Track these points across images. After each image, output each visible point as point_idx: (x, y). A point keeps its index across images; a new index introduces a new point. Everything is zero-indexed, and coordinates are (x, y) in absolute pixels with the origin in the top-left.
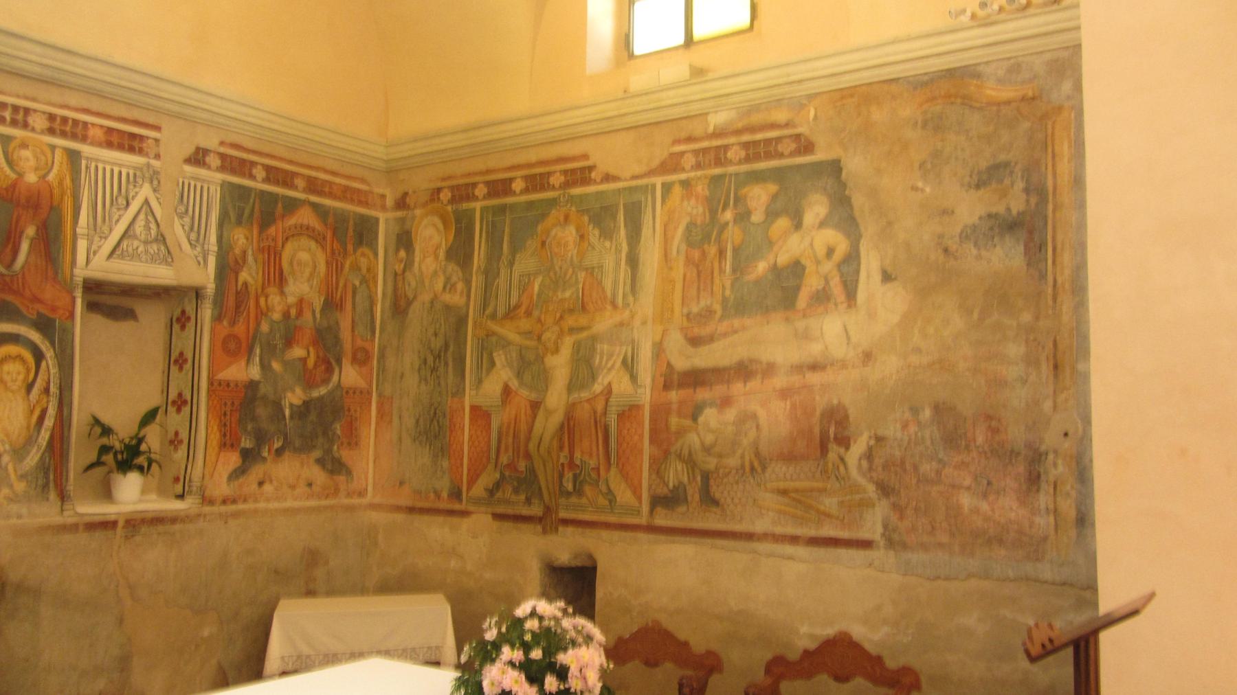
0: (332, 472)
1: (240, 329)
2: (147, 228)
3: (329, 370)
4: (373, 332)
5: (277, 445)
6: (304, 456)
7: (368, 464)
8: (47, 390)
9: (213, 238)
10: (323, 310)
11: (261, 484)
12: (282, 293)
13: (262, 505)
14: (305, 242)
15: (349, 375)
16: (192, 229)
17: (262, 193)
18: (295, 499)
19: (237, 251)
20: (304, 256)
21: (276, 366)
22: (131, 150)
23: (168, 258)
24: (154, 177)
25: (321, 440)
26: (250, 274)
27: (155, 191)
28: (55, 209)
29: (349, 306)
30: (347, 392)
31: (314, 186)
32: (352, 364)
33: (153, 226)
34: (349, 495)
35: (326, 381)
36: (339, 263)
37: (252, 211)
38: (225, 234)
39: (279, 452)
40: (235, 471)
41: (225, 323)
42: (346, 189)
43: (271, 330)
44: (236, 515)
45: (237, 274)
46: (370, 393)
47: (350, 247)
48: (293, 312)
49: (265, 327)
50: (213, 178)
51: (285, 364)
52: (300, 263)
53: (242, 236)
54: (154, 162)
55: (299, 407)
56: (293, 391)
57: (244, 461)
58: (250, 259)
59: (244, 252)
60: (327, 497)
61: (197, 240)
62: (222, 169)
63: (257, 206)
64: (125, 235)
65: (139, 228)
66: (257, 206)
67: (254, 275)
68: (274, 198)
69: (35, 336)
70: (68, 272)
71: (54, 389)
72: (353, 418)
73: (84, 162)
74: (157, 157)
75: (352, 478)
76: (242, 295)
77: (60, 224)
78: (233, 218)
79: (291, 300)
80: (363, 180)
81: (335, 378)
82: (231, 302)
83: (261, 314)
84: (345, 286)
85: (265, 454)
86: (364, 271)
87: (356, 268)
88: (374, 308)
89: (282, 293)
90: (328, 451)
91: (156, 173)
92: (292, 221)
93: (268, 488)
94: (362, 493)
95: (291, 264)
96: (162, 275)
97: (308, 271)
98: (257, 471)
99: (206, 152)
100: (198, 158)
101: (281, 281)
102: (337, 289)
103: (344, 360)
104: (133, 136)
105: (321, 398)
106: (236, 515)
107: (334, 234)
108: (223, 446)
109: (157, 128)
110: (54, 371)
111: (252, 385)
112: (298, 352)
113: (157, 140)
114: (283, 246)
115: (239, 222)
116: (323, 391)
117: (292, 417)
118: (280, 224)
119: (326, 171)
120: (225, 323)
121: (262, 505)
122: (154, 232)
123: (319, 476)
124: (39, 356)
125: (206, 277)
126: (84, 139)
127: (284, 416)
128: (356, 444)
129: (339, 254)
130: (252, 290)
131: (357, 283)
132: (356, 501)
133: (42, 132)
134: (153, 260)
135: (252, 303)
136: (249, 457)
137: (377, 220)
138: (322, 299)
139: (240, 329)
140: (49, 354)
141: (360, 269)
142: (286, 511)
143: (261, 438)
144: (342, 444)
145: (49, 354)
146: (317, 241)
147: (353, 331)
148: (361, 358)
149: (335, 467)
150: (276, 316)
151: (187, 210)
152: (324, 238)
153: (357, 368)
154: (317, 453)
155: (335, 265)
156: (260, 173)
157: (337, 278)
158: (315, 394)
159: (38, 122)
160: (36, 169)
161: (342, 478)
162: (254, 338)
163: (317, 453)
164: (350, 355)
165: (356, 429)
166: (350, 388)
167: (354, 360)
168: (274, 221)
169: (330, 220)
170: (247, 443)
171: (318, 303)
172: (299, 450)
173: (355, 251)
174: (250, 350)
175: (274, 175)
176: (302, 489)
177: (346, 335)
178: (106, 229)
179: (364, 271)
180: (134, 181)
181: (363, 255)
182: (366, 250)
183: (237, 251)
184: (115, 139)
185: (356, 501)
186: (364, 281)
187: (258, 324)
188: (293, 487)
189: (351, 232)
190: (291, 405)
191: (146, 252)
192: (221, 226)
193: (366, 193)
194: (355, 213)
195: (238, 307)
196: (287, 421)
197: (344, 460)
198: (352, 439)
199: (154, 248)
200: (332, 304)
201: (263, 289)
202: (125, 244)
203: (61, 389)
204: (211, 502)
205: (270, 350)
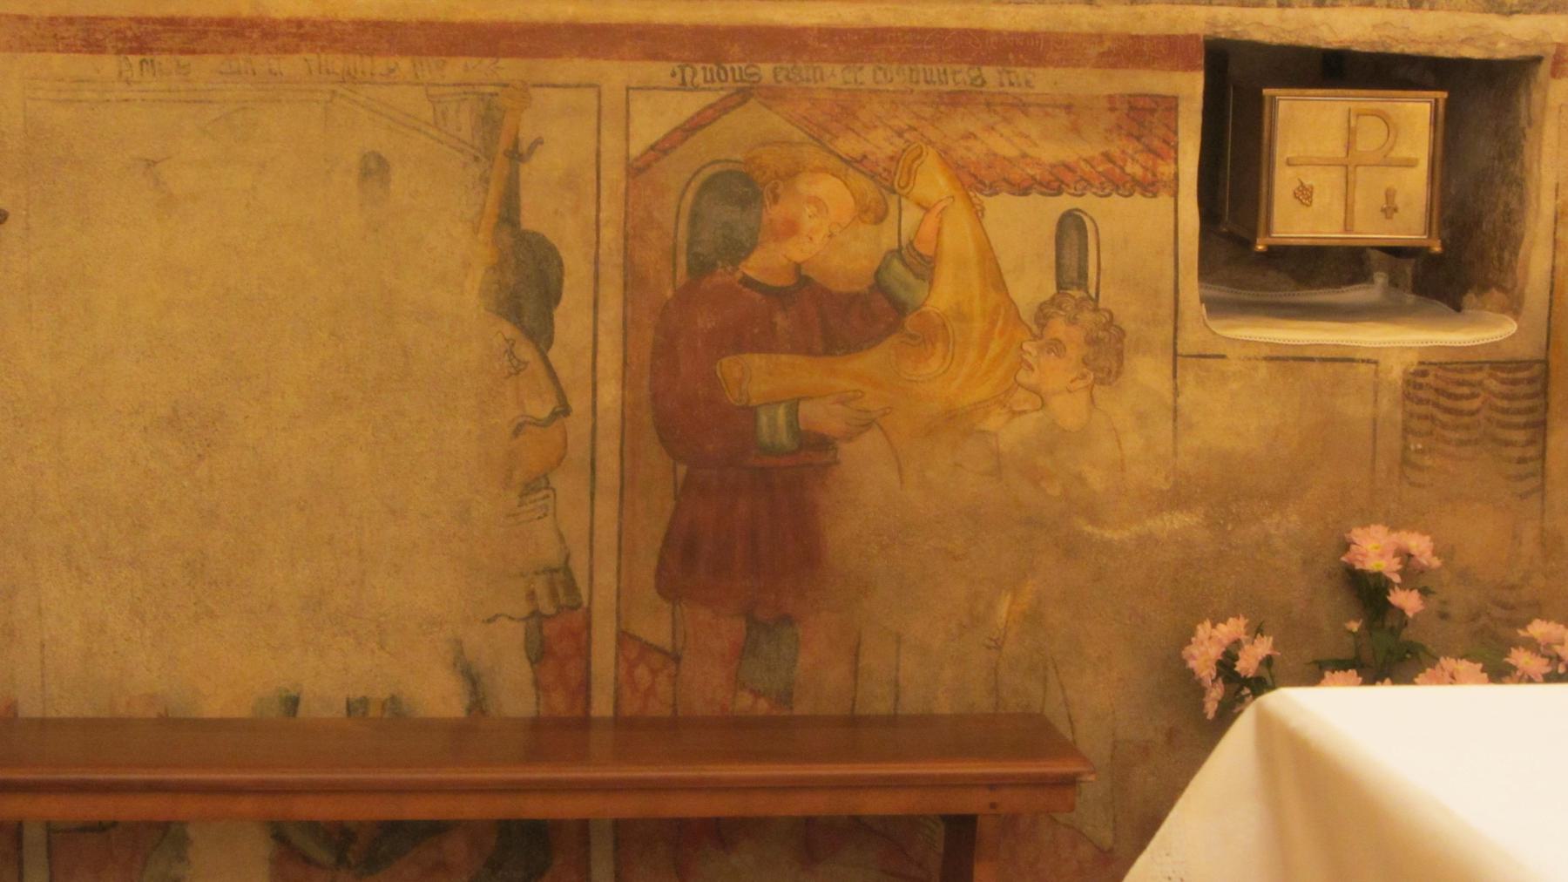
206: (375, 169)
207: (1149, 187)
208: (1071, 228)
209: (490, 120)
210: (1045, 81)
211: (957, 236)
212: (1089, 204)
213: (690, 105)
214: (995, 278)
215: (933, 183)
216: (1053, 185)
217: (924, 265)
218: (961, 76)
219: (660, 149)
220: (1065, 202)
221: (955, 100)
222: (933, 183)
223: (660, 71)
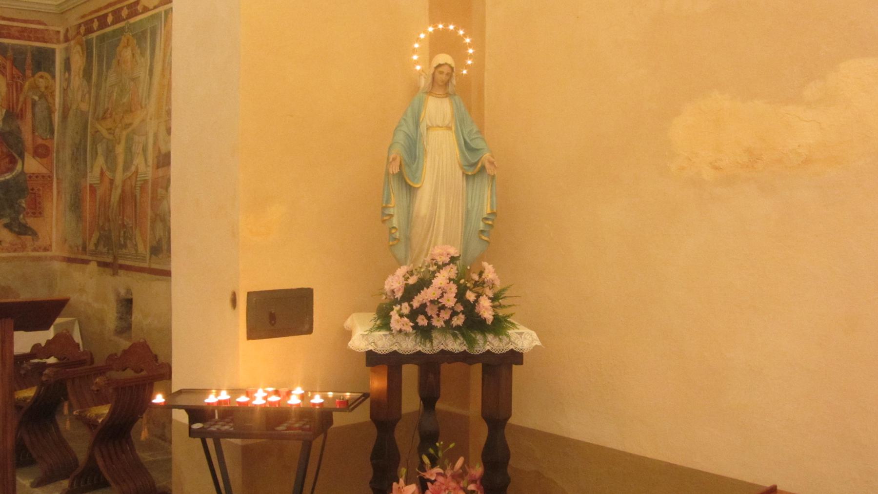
0: (19, 234)
3: (13, 162)
4: (52, 132)
7: (51, 227)
15: (32, 165)
25: (8, 211)
29: (29, 115)
30: (30, 177)
32: (33, 157)
34: (35, 250)
35: (9, 170)
36: (19, 84)
42: (24, 30)
46: (50, 177)
47: (29, 73)
60: (15, 251)
72: (37, 195)
75: (38, 237)
80: (39, 23)
81: (19, 167)
84: (25, 102)
87: (35, 87)
88: (53, 115)
94: (46, 250)
102: (17, 105)
103: (26, 154)
107: (14, 62)
116: (8, 176)
128: (40, 213)
129: (19, 78)
137: (53, 51)
144: (28, 213)
147: (33, 133)
148: (42, 152)
149: (23, 230)
152: (4, 67)
153: (38, 159)
157: (17, 95)
161: (29, 237)
163: (6, 220)
165: (40, 203)
166: (33, 174)
169: (10, 54)
173: (33, 75)
179: (43, 89)
181: (42, 77)
186: (42, 96)
193: (42, 31)
194: (32, 47)
198: (37, 210)
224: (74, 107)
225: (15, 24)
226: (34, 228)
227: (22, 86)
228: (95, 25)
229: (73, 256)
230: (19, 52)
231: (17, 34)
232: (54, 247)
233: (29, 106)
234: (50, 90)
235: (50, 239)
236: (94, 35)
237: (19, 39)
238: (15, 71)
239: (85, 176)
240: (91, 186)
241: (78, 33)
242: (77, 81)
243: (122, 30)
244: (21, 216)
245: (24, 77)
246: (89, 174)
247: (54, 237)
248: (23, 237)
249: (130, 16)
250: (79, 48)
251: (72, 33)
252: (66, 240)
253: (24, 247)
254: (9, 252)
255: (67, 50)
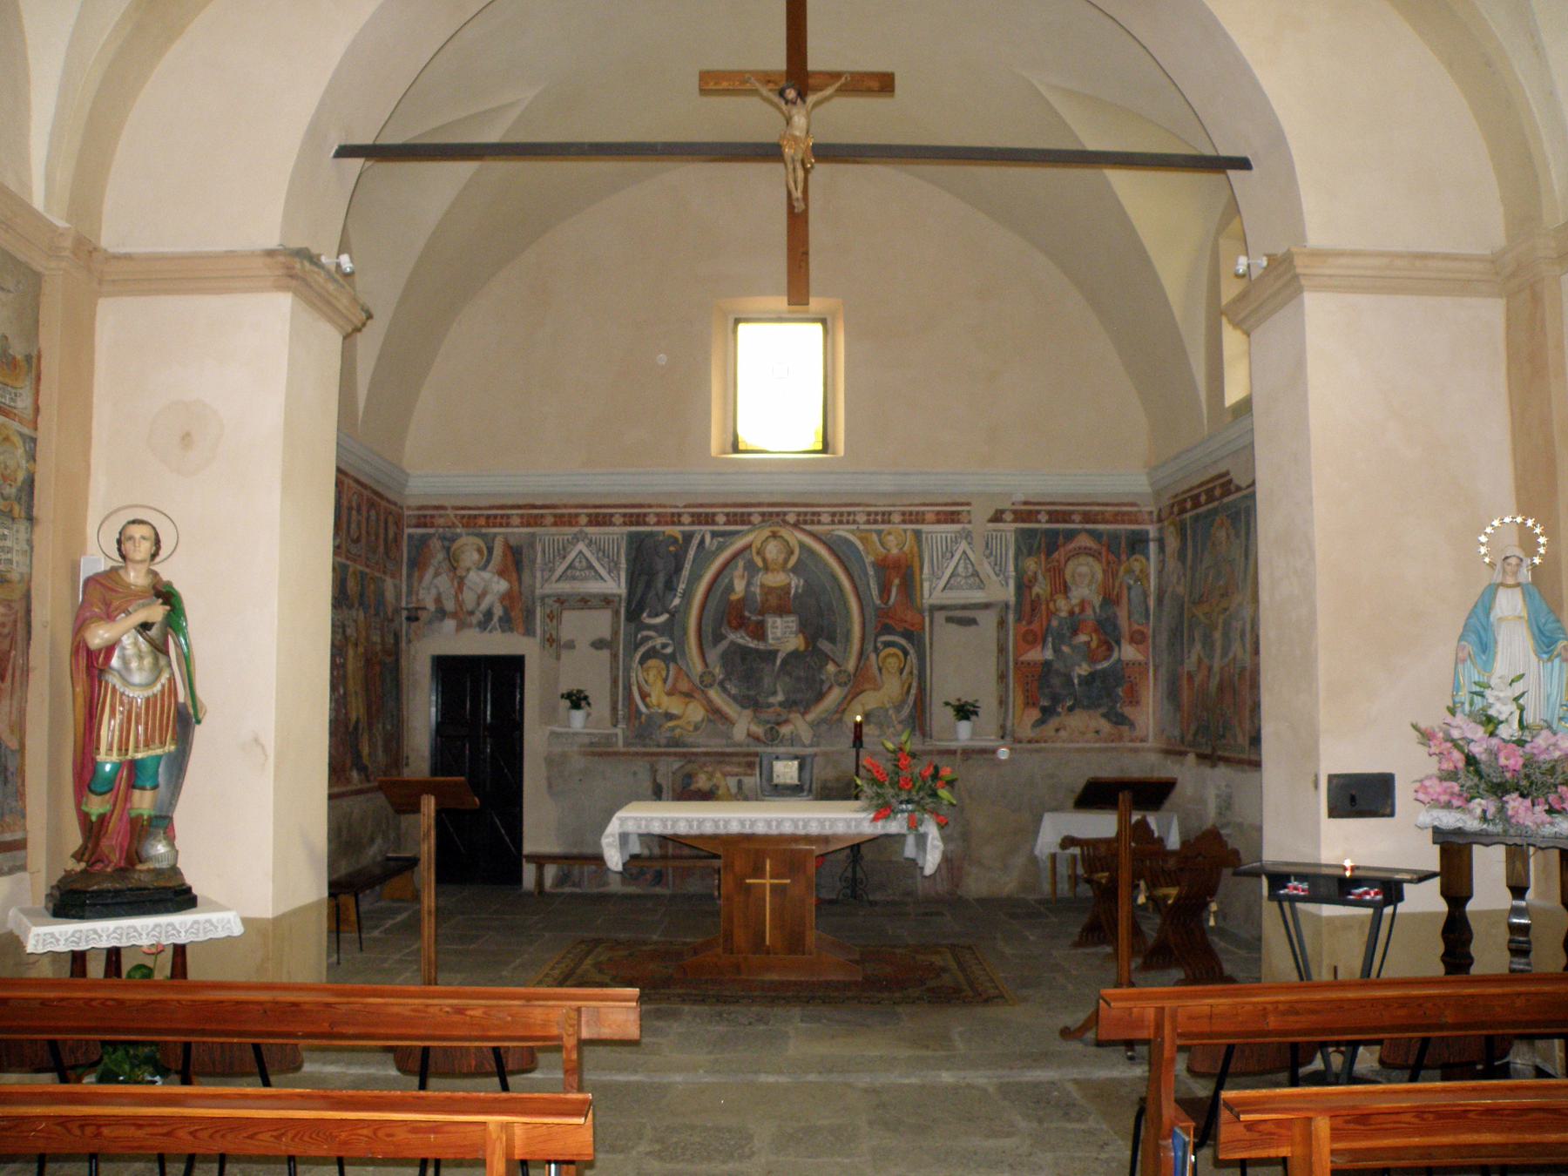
0: (1117, 723)
1: (1035, 626)
2: (966, 568)
3: (1110, 649)
4: (1147, 616)
5: (1069, 703)
6: (1091, 712)
8: (911, 673)
9: (1011, 567)
10: (1101, 606)
11: (1057, 730)
12: (1067, 598)
13: (1059, 745)
14: (1082, 559)
16: (996, 564)
17: (1046, 531)
18: (1086, 742)
19: (1030, 573)
20: (1084, 569)
21: (1065, 649)
22: (953, 522)
23: (981, 586)
24: (968, 536)
26: (1041, 588)
27: (969, 544)
28: (910, 567)
29: (1124, 600)
30: (1127, 664)
31: (1088, 518)
33: (969, 566)
34: (1132, 741)
35: (1106, 658)
37: (1040, 544)
38: (1020, 564)
39: (1071, 709)
40: (1037, 721)
41: (1024, 623)
42: (1117, 514)
43: (1060, 624)
44: (1037, 751)
45: (1030, 588)
47: (1124, 557)
48: (1077, 610)
49: (1055, 623)
50: (1009, 528)
51: (1073, 648)
52: (1080, 575)
53: (1032, 562)
54: (967, 526)
55: (1086, 677)
56: (1080, 666)
57: (1043, 715)
58: (1040, 577)
59: (1035, 573)
60: (1113, 741)
61: (1000, 571)
62: (1014, 521)
63: (1043, 540)
64: (953, 575)
65: (961, 569)
66: (1043, 540)
67: (1044, 586)
68: (1056, 533)
69: (903, 642)
70: (918, 600)
71: (915, 672)
73: (924, 536)
74: (970, 522)
76: (1035, 605)
77: (912, 575)
78: (1025, 551)
79: (1075, 601)
81: (1115, 655)
82: (1027, 608)
83: (1051, 614)
84: (1120, 587)
85: (1060, 710)
86: (1137, 573)
87: (1130, 571)
89: (1067, 598)
90: (1113, 707)
91: (969, 532)
92: (1072, 546)
93: (1063, 734)
94: (1142, 740)
95: (1073, 576)
96: (978, 596)
97: (1086, 582)
98: (1054, 722)
99: (1002, 512)
100: (997, 517)
101: (1065, 589)
103: (1123, 641)
104: (953, 513)
105: (1104, 671)
106: (1037, 751)
107: (1109, 549)
108: (1027, 704)
109: (968, 504)
110: (915, 661)
111: (1047, 664)
112: (1083, 638)
113: (969, 512)
114: (1066, 562)
115: (1030, 554)
116: (1105, 664)
117: (1080, 684)
118: (1062, 550)
119: (1099, 504)
120: (1024, 623)
121: (1059, 745)
122: (970, 570)
123: (1105, 726)
124: (906, 653)
125: (1009, 594)
126: (923, 522)
127: (1073, 684)
130: (1043, 598)
131: (1132, 582)
132: (1138, 745)
133: (899, 523)
134: (971, 587)
135: (1044, 607)
136: (1047, 713)
138: (1101, 599)
139: (1035, 626)
140: (912, 651)
141: (1133, 572)
142: (1078, 750)
143: (1056, 699)
145: (912, 651)
146: (1093, 556)
147: (1129, 618)
148: (1138, 638)
149: (1119, 720)
150: (1063, 614)
151: (991, 553)
152: (1100, 554)
154: (1103, 710)
155: (1111, 572)
156: (1043, 517)
158: (1099, 667)
159: (896, 518)
160: (897, 545)
161: (1127, 728)
162: (1047, 630)
163: (1103, 710)
164: (1127, 637)
165: (1137, 691)
167: (1132, 640)
168: (1057, 549)
170: (1045, 703)
171: (1097, 601)
172: (1088, 707)
173: (1128, 559)
174: (1044, 641)
175: (1054, 516)
176: (1091, 735)
177: (1123, 622)
178: (940, 574)
179: (1137, 573)
180: (956, 541)
181: (1136, 560)
182: (1137, 556)
183: (1030, 573)
184: (942, 517)
185: (1138, 745)
187: (1049, 621)
188: (1083, 733)
189: (1123, 544)
190: (1079, 676)
191: (967, 583)
192: (1016, 558)
194: (1126, 530)
195: (1033, 610)
196: (1077, 687)
197: (1126, 714)
198: (1134, 699)
199: (971, 580)
200: (1110, 600)
201: (1052, 595)
202: (952, 581)
203: (919, 673)
204: (1020, 742)
205: (1060, 639)
206: (635, 774)
207: (751, 775)
208: (740, 782)
209: (652, 766)
210: (735, 759)
211: (723, 783)
212: (742, 778)
213: (682, 763)
214: (728, 790)
215: (718, 775)
216: (737, 775)
217: (718, 788)
218: (722, 759)
219: (677, 770)
220: (738, 778)
221: (720, 762)
222: (718, 775)
223: (677, 759)
224: (1170, 590)
225: (1109, 509)
226: (1132, 717)
227: (1117, 571)
228: (1189, 505)
229: (1170, 747)
230: (1114, 537)
231: (1111, 518)
232: (1151, 738)
233: (1125, 592)
234: (1145, 574)
235: (1147, 729)
236: (1187, 516)
237: (1111, 523)
238: (1111, 557)
239: (1182, 663)
240: (1189, 673)
241: (1171, 513)
242: (1172, 564)
243: (1215, 511)
244: (1118, 705)
245: (1120, 562)
246: (1187, 661)
247: (1151, 729)
248: (1120, 727)
249: (1223, 495)
250: (1172, 529)
251: (1164, 515)
252: (1163, 731)
253: (1121, 738)
254: (1106, 741)
255: (1161, 530)
